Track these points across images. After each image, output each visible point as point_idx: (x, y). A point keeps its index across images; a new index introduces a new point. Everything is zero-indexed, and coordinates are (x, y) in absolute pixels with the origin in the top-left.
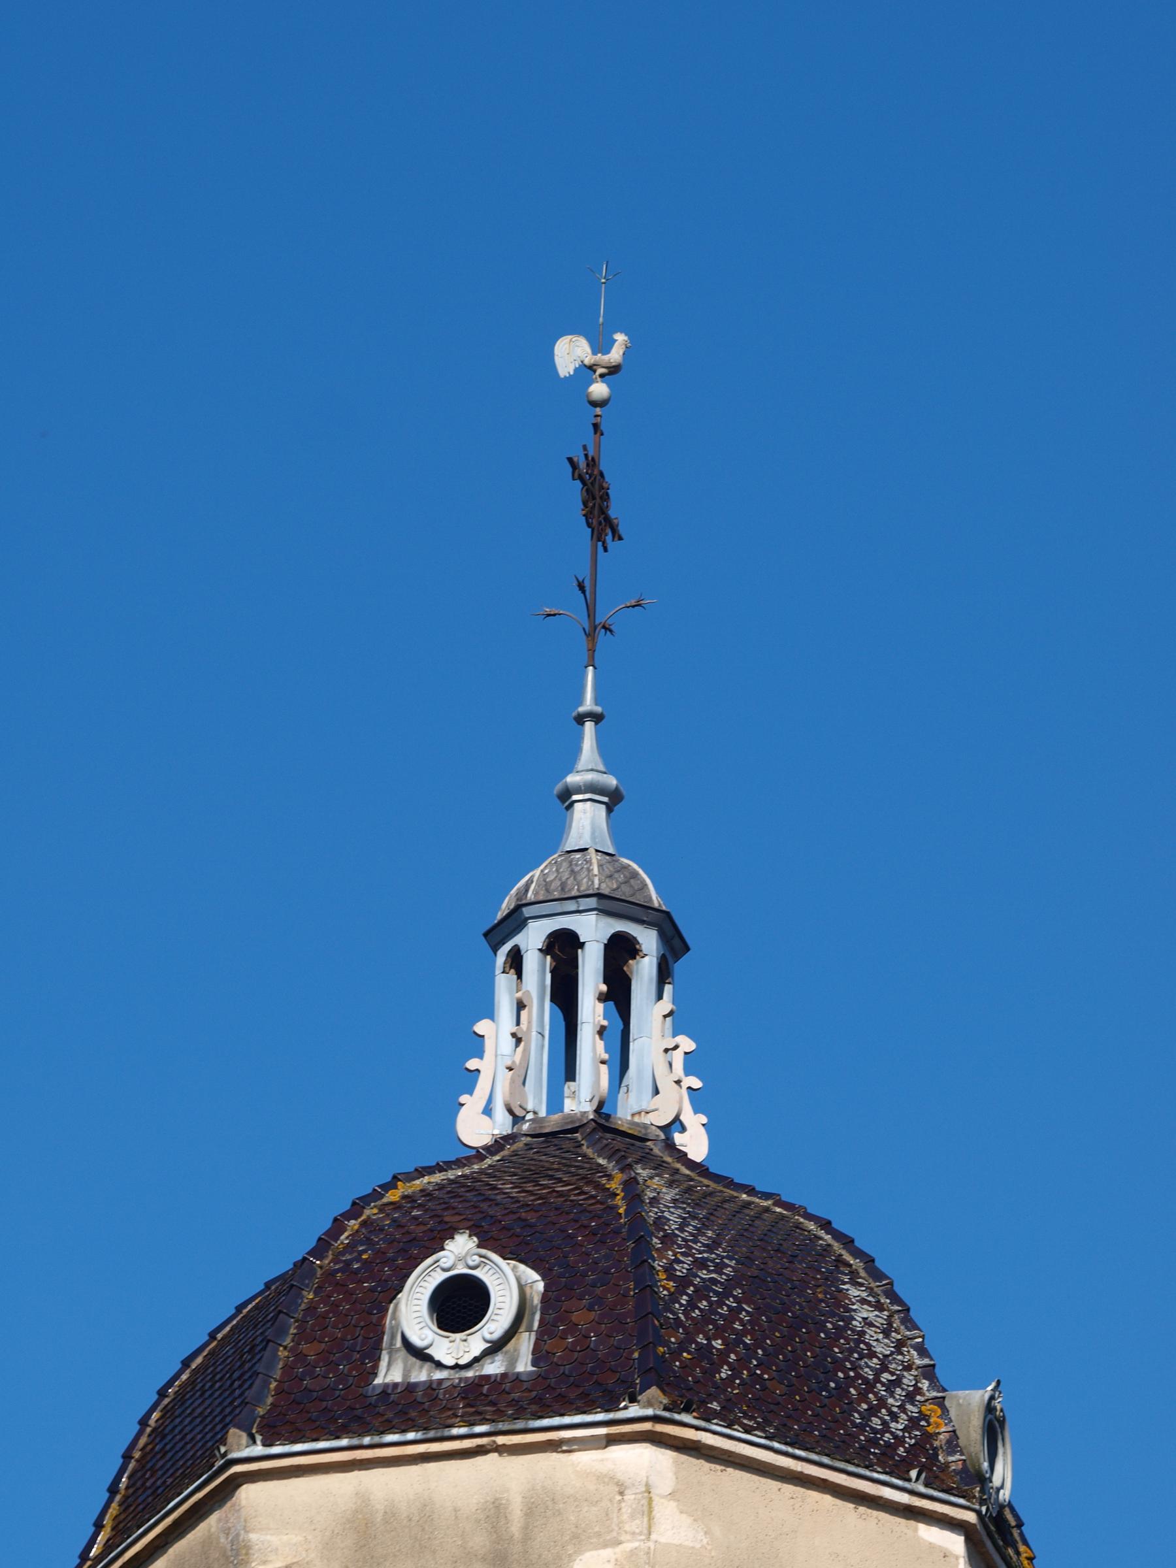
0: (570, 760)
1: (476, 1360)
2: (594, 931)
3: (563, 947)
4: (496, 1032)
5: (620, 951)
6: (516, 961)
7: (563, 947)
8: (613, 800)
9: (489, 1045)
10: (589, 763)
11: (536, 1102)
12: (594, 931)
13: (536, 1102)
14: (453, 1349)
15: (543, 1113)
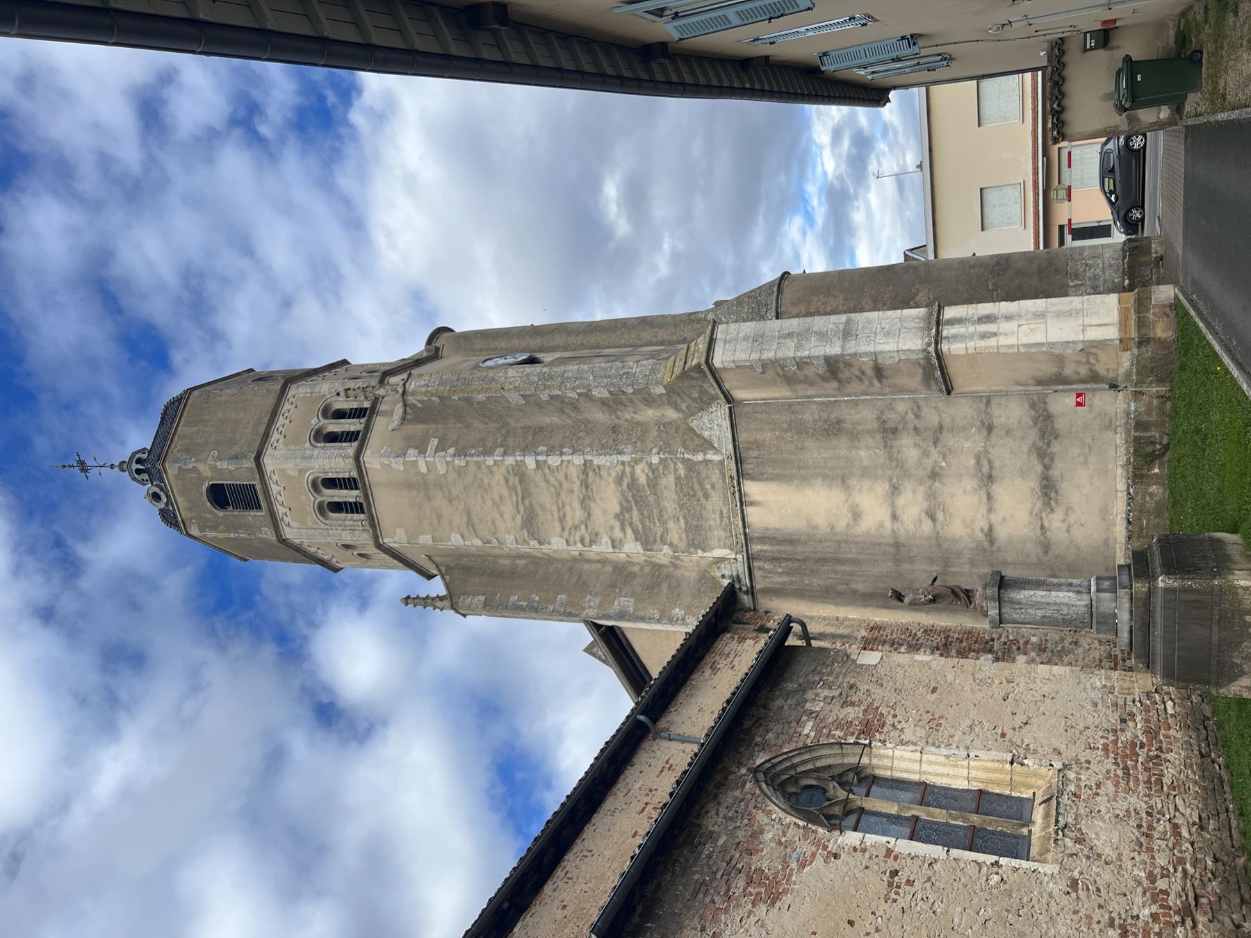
2: (135, 466)
3: (138, 471)
12: (135, 466)
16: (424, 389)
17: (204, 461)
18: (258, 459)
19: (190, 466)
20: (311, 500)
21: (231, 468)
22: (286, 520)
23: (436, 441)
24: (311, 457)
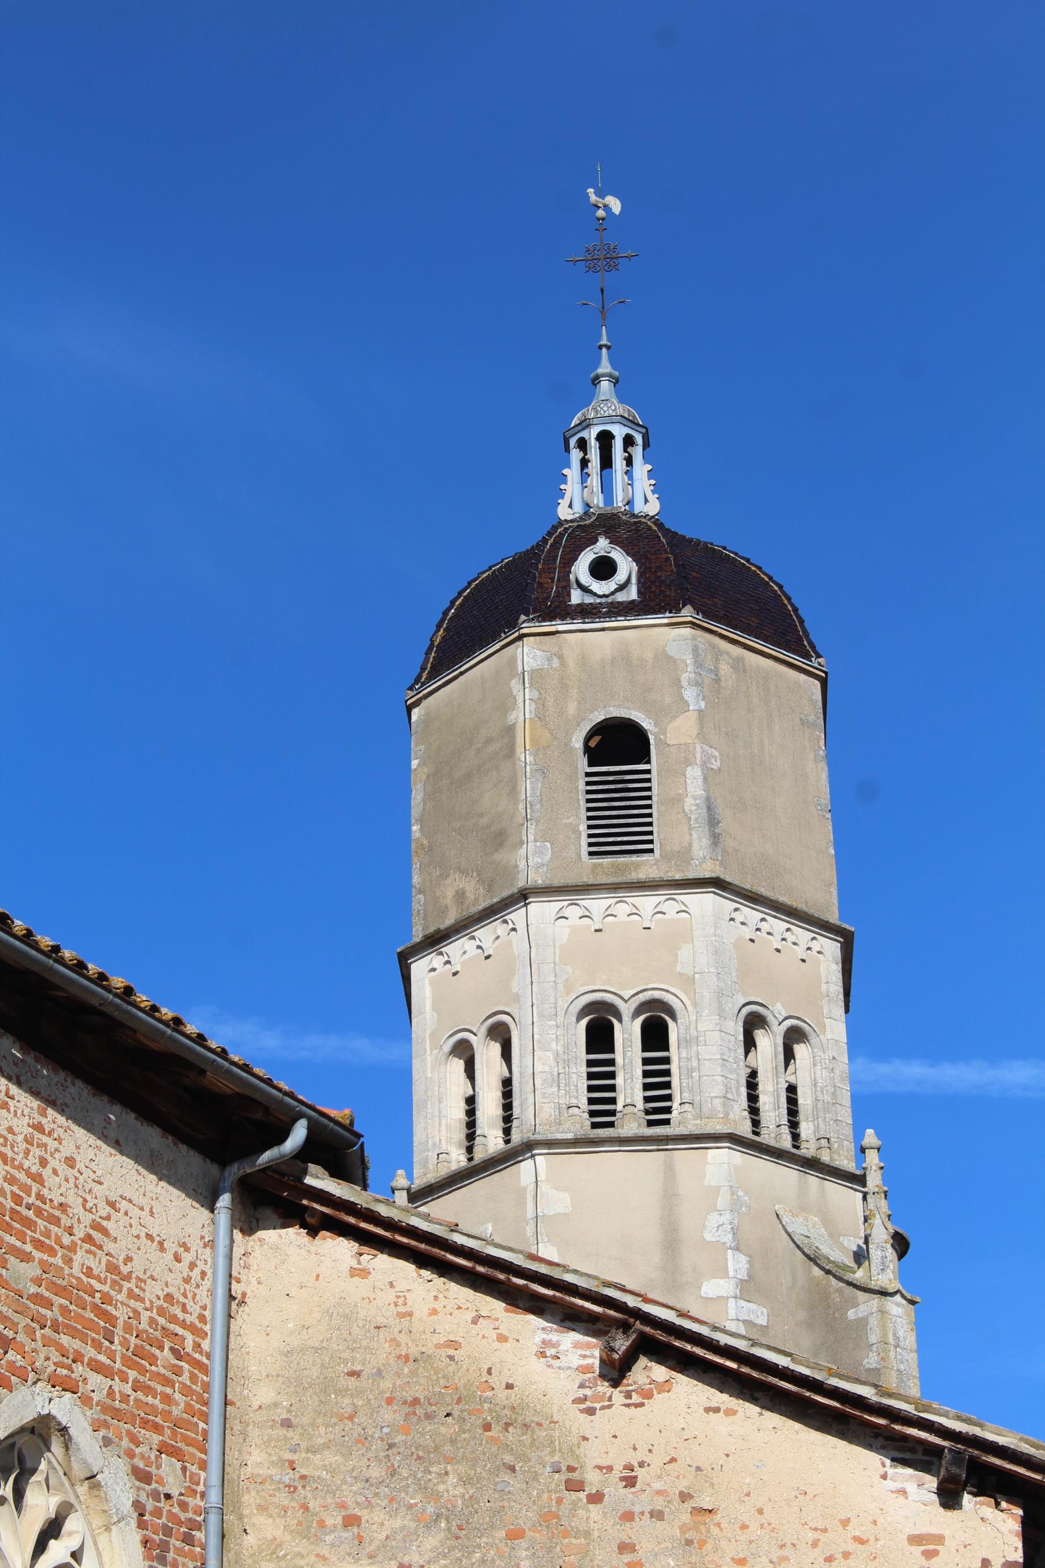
0: (597, 362)
1: (613, 593)
2: (619, 432)
3: (606, 438)
4: (573, 473)
5: (629, 441)
6: (582, 444)
7: (606, 438)
8: (616, 382)
9: (569, 478)
10: (605, 367)
11: (598, 501)
13: (598, 501)
14: (600, 587)
15: (601, 505)
16: (891, 1339)
17: (702, 736)
18: (717, 884)
19: (690, 694)
20: (626, 991)
21: (689, 804)
22: (573, 912)
23: (762, 1321)
24: (722, 1015)
